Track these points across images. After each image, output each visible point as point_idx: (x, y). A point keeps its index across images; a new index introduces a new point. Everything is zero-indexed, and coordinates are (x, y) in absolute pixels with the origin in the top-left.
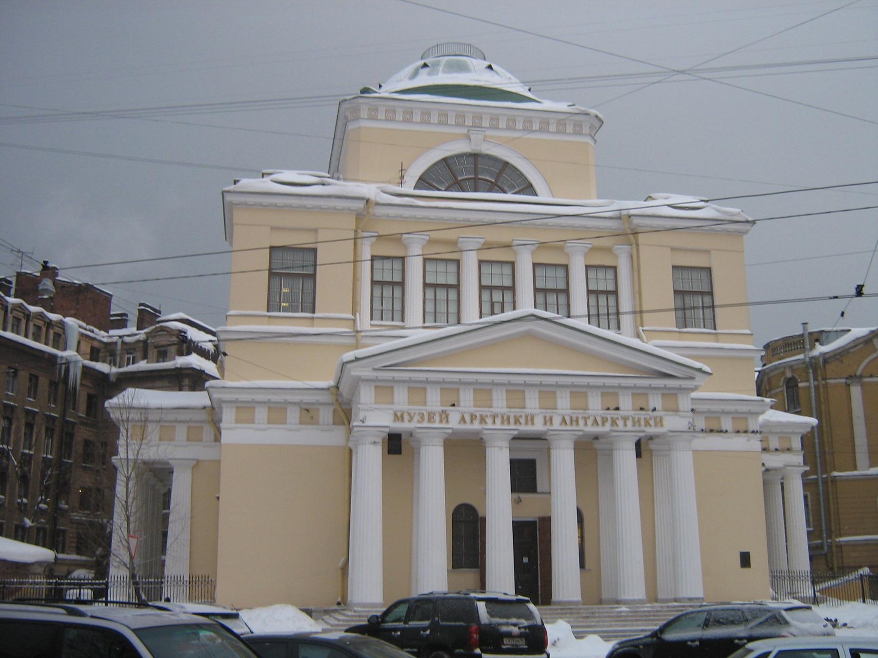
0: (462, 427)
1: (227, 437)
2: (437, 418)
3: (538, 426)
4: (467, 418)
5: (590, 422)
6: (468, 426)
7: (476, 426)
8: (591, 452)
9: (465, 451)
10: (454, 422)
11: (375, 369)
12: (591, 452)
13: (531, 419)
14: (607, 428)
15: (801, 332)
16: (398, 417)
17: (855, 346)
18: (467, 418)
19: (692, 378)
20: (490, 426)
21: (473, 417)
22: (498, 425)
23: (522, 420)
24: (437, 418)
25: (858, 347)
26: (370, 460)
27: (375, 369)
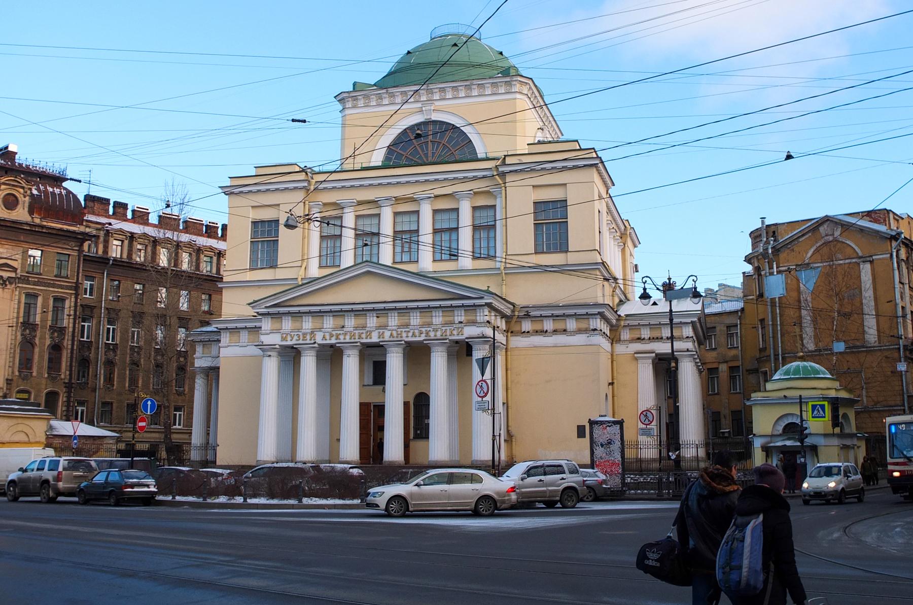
0: (325, 342)
1: (224, 352)
2: (308, 337)
3: (375, 339)
4: (327, 337)
5: (410, 334)
6: (328, 342)
7: (333, 341)
8: (416, 355)
9: (331, 357)
10: (319, 339)
11: (266, 307)
12: (416, 355)
13: (369, 334)
14: (423, 337)
15: (760, 226)
16: (283, 339)
17: (803, 235)
18: (327, 337)
19: (482, 298)
20: (342, 341)
21: (331, 336)
22: (348, 340)
23: (364, 336)
24: (308, 337)
25: (807, 236)
26: (271, 366)
27: (266, 307)
